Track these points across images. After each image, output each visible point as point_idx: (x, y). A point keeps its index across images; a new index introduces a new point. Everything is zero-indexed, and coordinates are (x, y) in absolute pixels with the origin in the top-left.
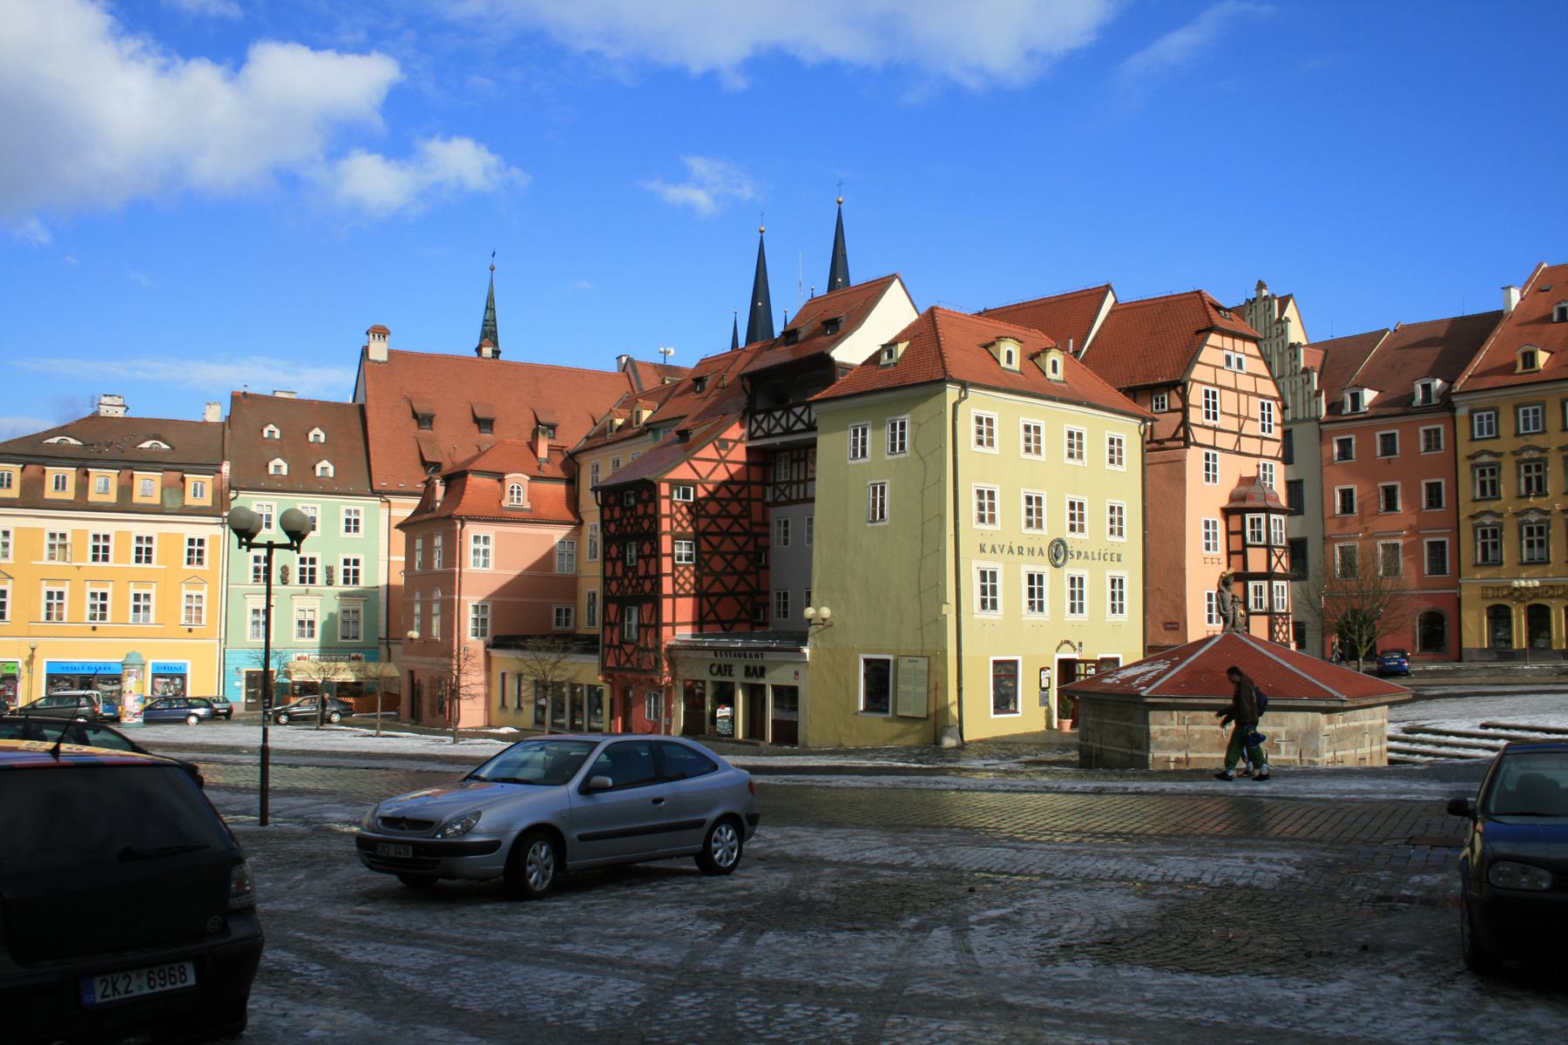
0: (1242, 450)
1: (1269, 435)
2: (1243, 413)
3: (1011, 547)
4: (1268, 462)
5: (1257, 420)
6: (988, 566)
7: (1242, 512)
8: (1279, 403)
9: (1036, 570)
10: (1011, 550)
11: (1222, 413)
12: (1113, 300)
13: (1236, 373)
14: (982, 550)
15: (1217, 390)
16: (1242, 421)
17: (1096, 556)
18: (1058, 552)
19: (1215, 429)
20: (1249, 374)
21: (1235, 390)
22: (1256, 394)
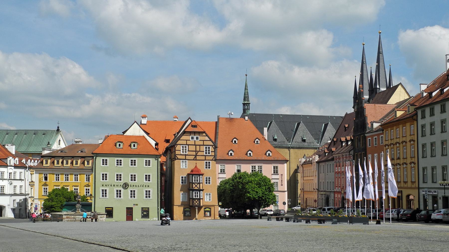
0: (197, 159)
1: (209, 155)
2: (198, 149)
3: (111, 185)
4: (208, 161)
6: (104, 188)
7: (193, 175)
8: (214, 146)
9: (119, 189)
10: (111, 185)
12: (191, 121)
13: (195, 141)
14: (103, 186)
15: (187, 146)
16: (197, 152)
17: (140, 186)
18: (126, 186)
19: (186, 155)
20: (200, 140)
21: (195, 145)
22: (204, 145)
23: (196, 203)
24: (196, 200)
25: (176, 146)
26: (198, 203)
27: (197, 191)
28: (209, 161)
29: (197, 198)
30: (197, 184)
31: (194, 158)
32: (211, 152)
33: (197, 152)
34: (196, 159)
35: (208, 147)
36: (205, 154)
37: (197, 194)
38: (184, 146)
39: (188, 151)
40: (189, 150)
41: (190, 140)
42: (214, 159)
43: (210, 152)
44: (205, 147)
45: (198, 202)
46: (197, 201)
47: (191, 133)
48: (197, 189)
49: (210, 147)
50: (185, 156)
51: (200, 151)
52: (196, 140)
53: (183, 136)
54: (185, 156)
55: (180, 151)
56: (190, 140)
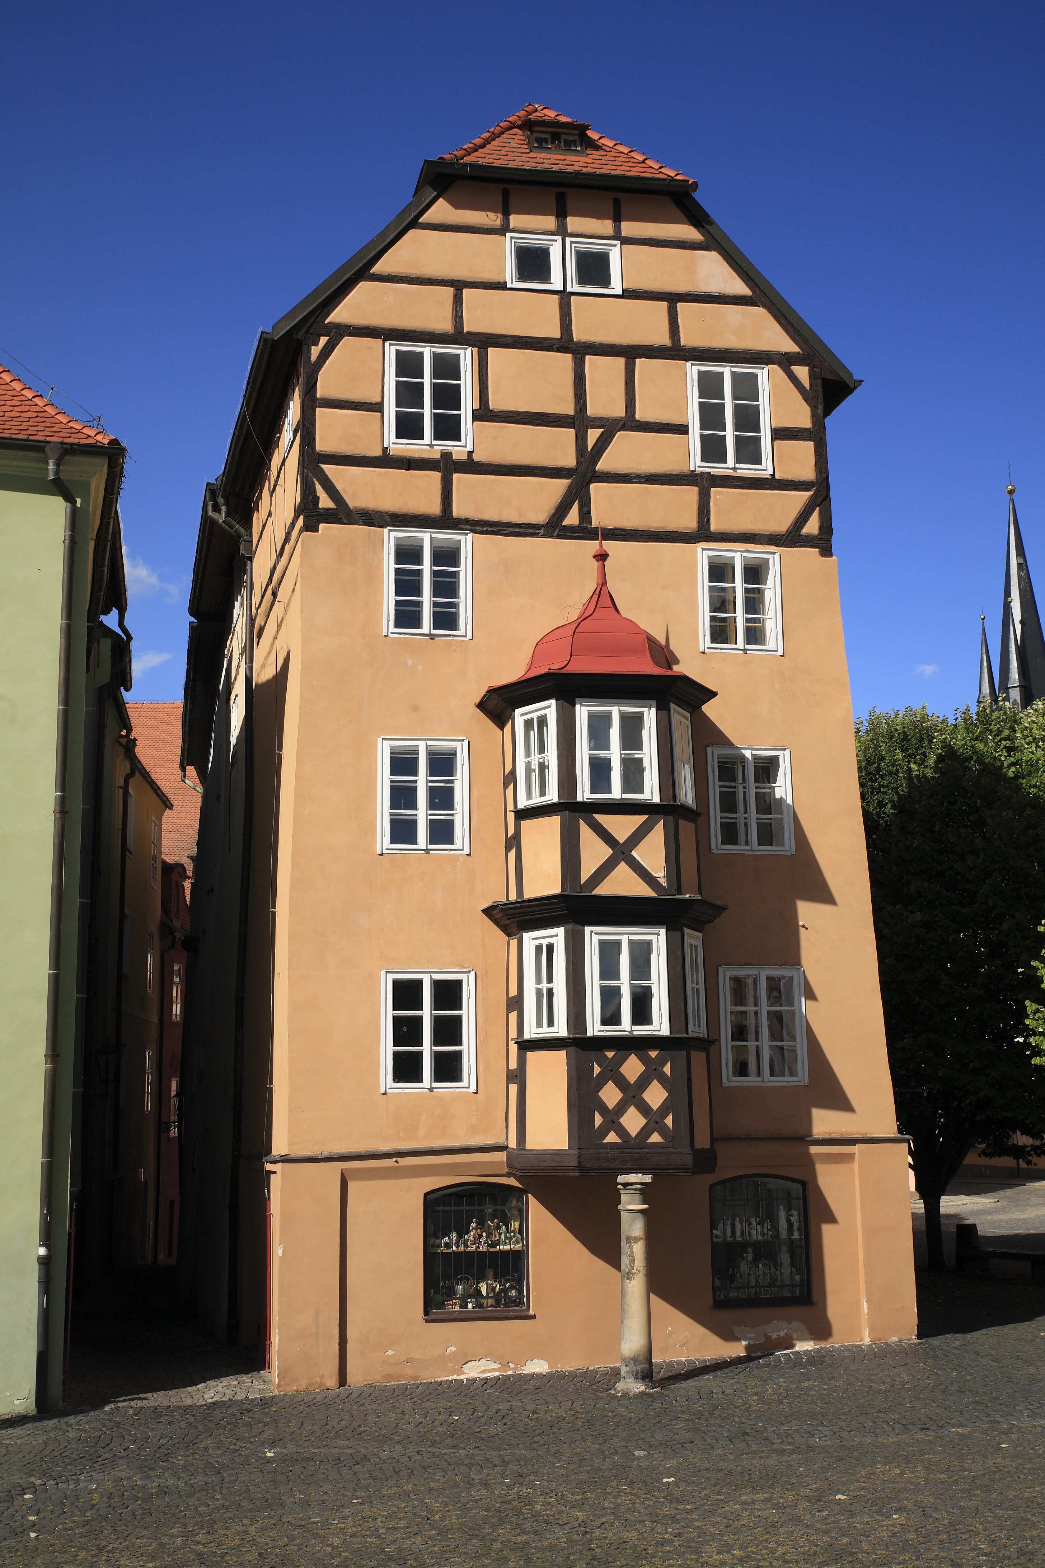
1: (747, 470)
5: (682, 429)
8: (802, 372)
11: (483, 414)
13: (564, 296)
15: (467, 356)
20: (628, 294)
23: (621, 1108)
24: (632, 1068)
25: (315, 351)
26: (665, 1108)
27: (640, 933)
28: (756, 552)
29: (641, 1030)
30: (639, 820)
31: (562, 509)
32: (779, 434)
33: (593, 435)
34: (585, 514)
35: (727, 371)
36: (696, 463)
37: (641, 967)
38: (427, 351)
39: (483, 414)
40: (494, 404)
41: (501, 286)
42: (812, 527)
43: (765, 435)
44: (692, 370)
45: (656, 1095)
46: (643, 1082)
47: (512, 201)
48: (643, 890)
49: (765, 375)
50: (436, 476)
51: (630, 423)
52: (573, 286)
53: (412, 233)
54: (436, 476)
55: (378, 407)
56: (501, 286)
